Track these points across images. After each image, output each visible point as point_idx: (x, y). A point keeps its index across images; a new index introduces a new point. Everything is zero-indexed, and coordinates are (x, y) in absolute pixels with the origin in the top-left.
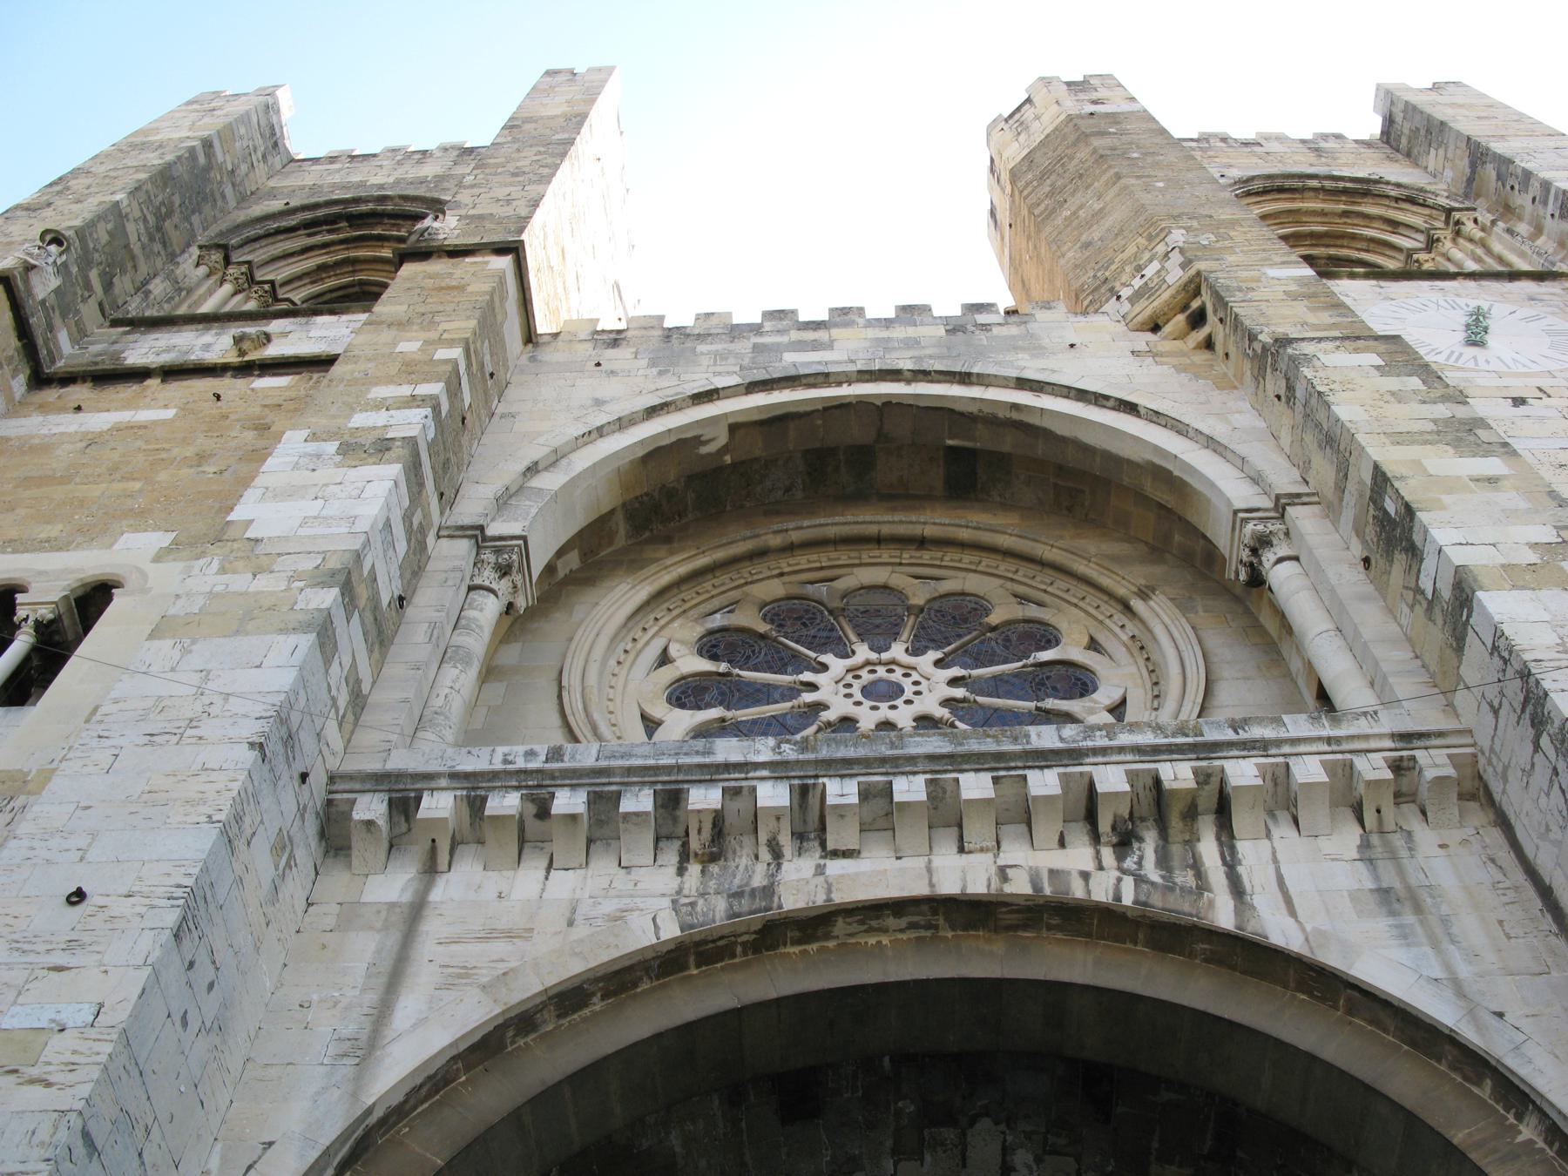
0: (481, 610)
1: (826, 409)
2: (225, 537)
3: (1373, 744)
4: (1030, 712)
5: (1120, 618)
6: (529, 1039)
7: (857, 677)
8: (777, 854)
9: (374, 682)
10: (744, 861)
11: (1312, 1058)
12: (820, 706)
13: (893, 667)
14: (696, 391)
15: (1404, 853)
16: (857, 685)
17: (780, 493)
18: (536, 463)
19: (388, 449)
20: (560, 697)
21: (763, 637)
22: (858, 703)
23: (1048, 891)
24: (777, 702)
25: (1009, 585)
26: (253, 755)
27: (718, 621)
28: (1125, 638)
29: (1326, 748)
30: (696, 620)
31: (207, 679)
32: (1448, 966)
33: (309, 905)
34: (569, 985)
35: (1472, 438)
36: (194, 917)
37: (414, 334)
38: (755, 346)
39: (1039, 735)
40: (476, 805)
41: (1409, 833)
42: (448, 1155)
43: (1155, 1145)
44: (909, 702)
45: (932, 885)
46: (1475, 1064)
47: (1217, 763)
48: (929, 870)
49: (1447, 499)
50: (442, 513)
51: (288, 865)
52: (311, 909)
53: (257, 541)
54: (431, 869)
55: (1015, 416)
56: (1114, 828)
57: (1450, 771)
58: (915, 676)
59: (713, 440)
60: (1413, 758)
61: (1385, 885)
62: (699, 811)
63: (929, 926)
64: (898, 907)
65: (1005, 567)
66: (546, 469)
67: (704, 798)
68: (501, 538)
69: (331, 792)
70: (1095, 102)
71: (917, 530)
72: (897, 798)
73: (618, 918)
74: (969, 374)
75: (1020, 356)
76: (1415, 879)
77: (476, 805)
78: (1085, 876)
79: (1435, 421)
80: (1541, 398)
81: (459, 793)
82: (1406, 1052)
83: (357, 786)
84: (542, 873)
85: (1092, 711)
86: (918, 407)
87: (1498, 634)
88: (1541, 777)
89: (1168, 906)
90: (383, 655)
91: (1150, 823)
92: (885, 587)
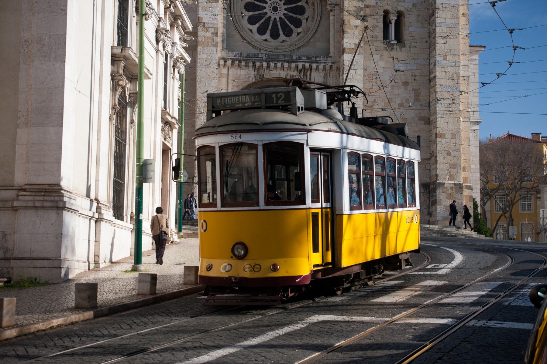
3: (329, 63)
10: (261, 70)
12: (266, 13)
15: (328, 77)
16: (272, 7)
22: (271, 12)
41: (330, 74)
44: (279, 13)
53: (204, 23)
54: (228, 69)
57: (336, 68)
58: (280, 6)
67: (258, 64)
73: (249, 77)
76: (328, 81)
78: (295, 76)
85: (304, 19)
87: (343, 61)
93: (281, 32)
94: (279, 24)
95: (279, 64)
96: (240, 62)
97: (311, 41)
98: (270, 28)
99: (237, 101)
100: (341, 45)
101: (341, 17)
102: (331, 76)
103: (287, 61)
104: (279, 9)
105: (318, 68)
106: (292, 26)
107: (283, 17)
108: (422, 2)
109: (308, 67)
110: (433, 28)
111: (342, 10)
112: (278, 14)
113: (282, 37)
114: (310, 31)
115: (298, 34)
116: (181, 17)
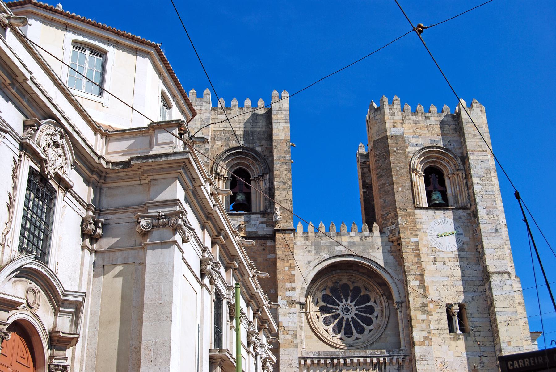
15: (402, 369)
16: (344, 308)
21: (331, 297)
22: (344, 313)
27: (324, 292)
37: (286, 264)
41: (403, 366)
44: (350, 313)
49: (417, 325)
58: (351, 308)
60: (405, 358)
67: (335, 361)
70: (394, 126)
77: (312, 362)
79: (421, 303)
87: (415, 353)
93: (354, 331)
94: (351, 323)
96: (319, 361)
97: (382, 336)
98: (343, 327)
99: (532, 363)
100: (411, 339)
101: (408, 313)
102: (404, 368)
105: (392, 361)
106: (363, 325)
107: (355, 317)
108: (480, 295)
109: (382, 361)
110: (494, 318)
111: (408, 307)
112: (350, 314)
113: (355, 334)
114: (381, 328)
115: (370, 331)
116: (268, 320)
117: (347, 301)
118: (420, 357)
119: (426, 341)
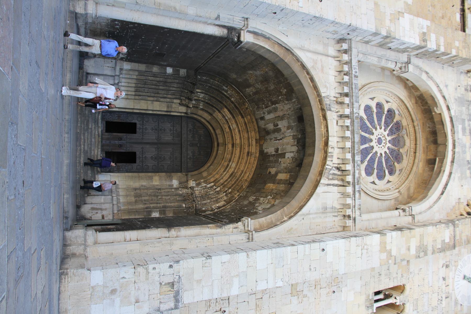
0: (391, 64)
1: (445, 133)
2: (400, 13)
3: (354, 213)
4: (374, 167)
5: (395, 187)
6: (306, 74)
7: (383, 137)
8: (337, 112)
9: (372, 45)
11: (299, 191)
12: (376, 129)
13: (385, 144)
14: (449, 106)
16: (381, 137)
17: (428, 126)
18: (428, 73)
19: (424, 42)
20: (377, 82)
21: (393, 121)
22: (377, 136)
23: (329, 154)
24: (378, 122)
25: (404, 168)
26: (349, 24)
27: (397, 112)
28: (390, 188)
29: (353, 205)
30: (397, 108)
31: (365, 14)
32: (312, 214)
33: (328, 38)
34: (314, 79)
35: (421, 251)
36: (319, 19)
38: (464, 119)
39: (359, 157)
40: (346, 63)
42: (287, 62)
43: (292, 174)
44: (377, 145)
45: (331, 136)
46: (297, 213)
47: (351, 186)
48: (334, 136)
50: (414, 55)
51: (333, 34)
52: (327, 39)
53: (399, 19)
54: (334, 57)
55: (442, 171)
56: (340, 167)
57: (347, 225)
58: (383, 147)
59: (437, 110)
60: (351, 220)
61: (327, 209)
62: (344, 99)
63: (325, 136)
64: (327, 131)
65: (409, 168)
66: (428, 76)
67: (347, 100)
68: (408, 67)
69: (348, 39)
71: (418, 151)
72: (346, 132)
73: (326, 87)
74: (453, 163)
75: (459, 174)
76: (329, 214)
77: (346, 63)
78: (332, 161)
79: (427, 245)
80: (445, 284)
81: (348, 60)
82: (299, 205)
83: (349, 44)
84: (334, 75)
85: (373, 178)
86: (445, 152)
88: (342, 235)
89: (325, 173)
90: (378, 46)
91: (341, 174)
92: (405, 145)
95: (348, 134)
98: (363, 134)
103: (354, 147)
104: (380, 146)
107: (374, 151)
117: (389, 141)
118: (366, 245)
119: (385, 254)
